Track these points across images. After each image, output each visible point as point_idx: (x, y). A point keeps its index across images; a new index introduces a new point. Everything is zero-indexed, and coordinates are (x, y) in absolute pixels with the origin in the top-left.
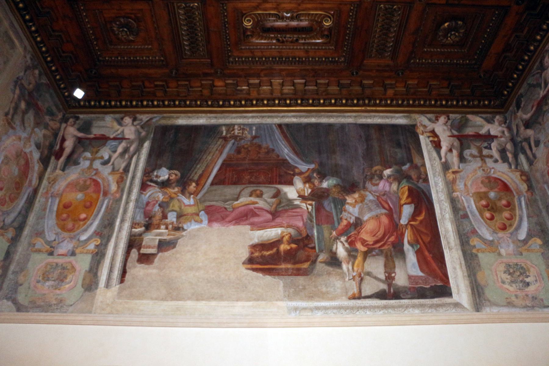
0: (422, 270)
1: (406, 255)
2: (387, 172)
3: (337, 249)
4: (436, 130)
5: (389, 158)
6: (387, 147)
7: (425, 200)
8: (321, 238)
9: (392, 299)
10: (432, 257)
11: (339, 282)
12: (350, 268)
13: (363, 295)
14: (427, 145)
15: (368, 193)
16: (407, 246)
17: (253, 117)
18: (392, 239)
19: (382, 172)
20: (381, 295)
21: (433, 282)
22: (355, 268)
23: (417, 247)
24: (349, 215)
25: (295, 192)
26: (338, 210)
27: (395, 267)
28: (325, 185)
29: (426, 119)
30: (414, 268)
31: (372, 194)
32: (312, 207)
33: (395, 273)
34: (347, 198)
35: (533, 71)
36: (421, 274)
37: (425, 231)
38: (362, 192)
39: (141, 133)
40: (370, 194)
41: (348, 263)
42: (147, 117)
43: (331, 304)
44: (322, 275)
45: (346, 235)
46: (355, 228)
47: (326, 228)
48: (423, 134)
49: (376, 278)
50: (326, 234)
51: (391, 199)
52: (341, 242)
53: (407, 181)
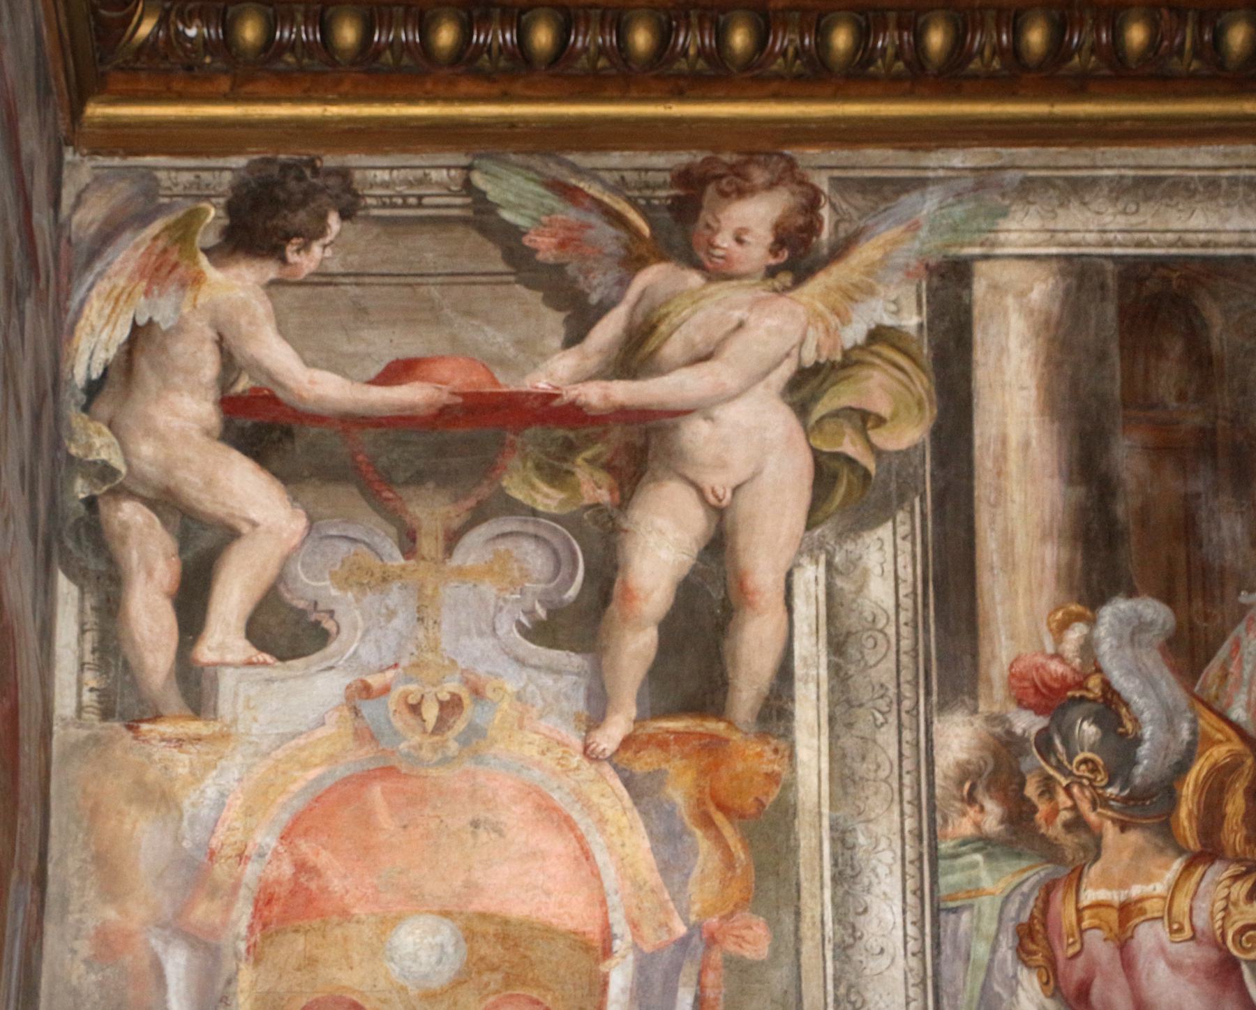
35: (574, 157)
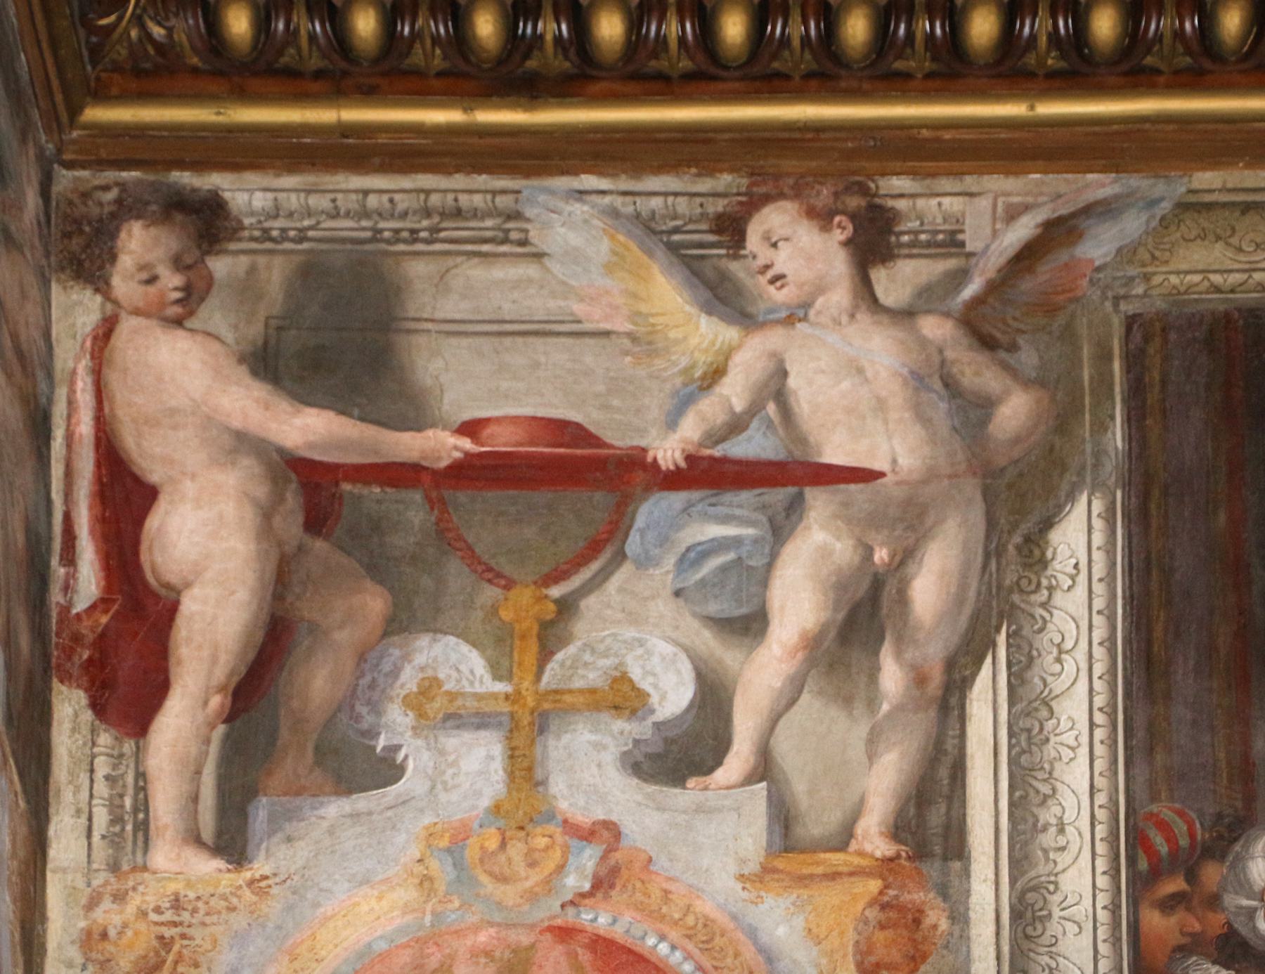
39: (986, 405)
42: (1012, 214)
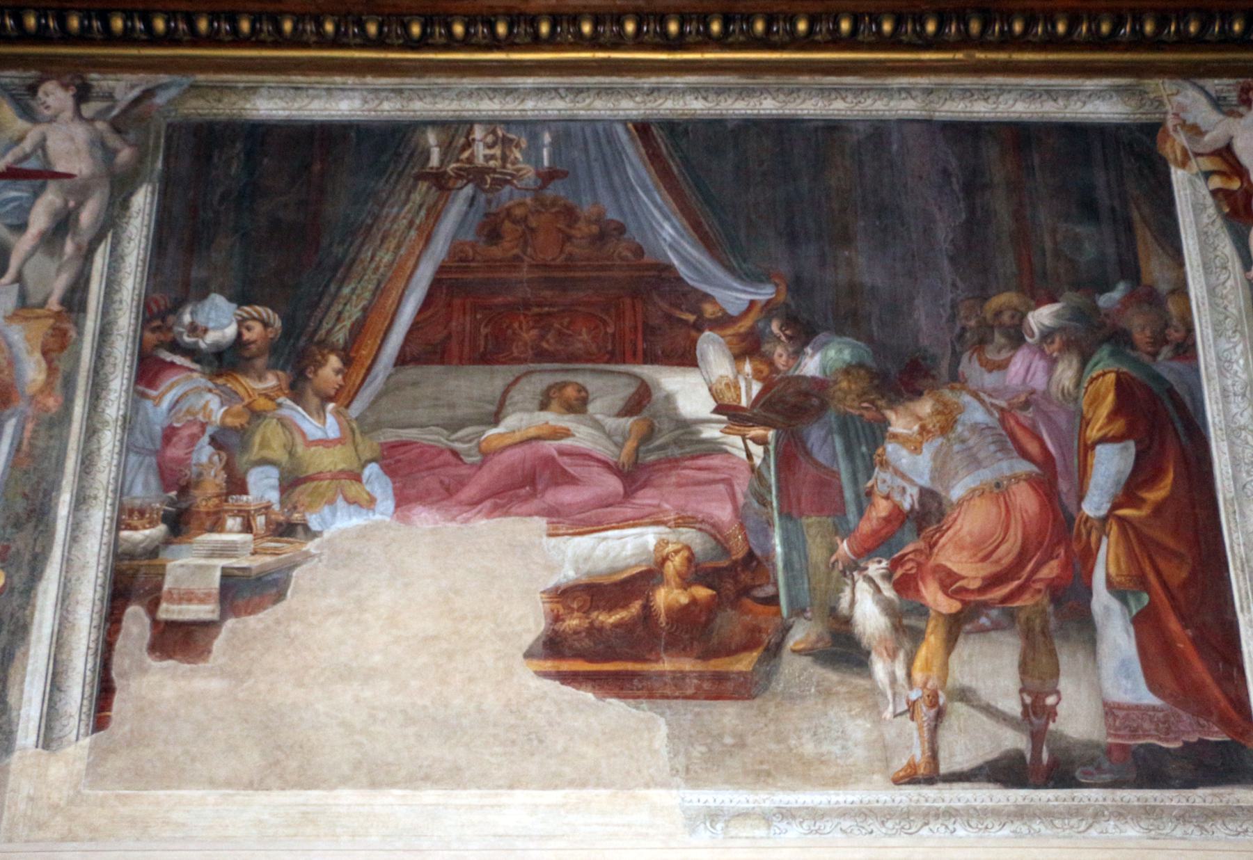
0: (1154, 685)
1: (1099, 630)
2: (1042, 317)
3: (853, 603)
4: (1239, 147)
5: (1049, 260)
6: (1044, 216)
7: (1179, 426)
8: (797, 566)
9: (1044, 785)
10: (1194, 641)
11: (860, 722)
12: (900, 672)
13: (943, 769)
14: (1198, 209)
15: (966, 398)
16: (1101, 599)
17: (540, 91)
18: (1050, 570)
19: (1023, 316)
20: (1006, 771)
21: (1193, 730)
22: (918, 676)
23: (1139, 600)
24: (899, 482)
25: (705, 391)
26: (859, 462)
27: (1056, 674)
28: (811, 365)
29: (1203, 100)
30: (1128, 677)
31: (982, 402)
32: (766, 451)
33: (1058, 693)
34: (891, 415)
36: (1150, 699)
37: (1170, 542)
38: (947, 394)
39: (115, 152)
40: (976, 403)
41: (893, 656)
42: (133, 87)
43: (834, 799)
44: (803, 698)
45: (887, 555)
46: (920, 530)
47: (813, 526)
48: (1183, 164)
49: (990, 711)
50: (816, 552)
51: (1049, 421)
52: (870, 580)
53: (1112, 354)
